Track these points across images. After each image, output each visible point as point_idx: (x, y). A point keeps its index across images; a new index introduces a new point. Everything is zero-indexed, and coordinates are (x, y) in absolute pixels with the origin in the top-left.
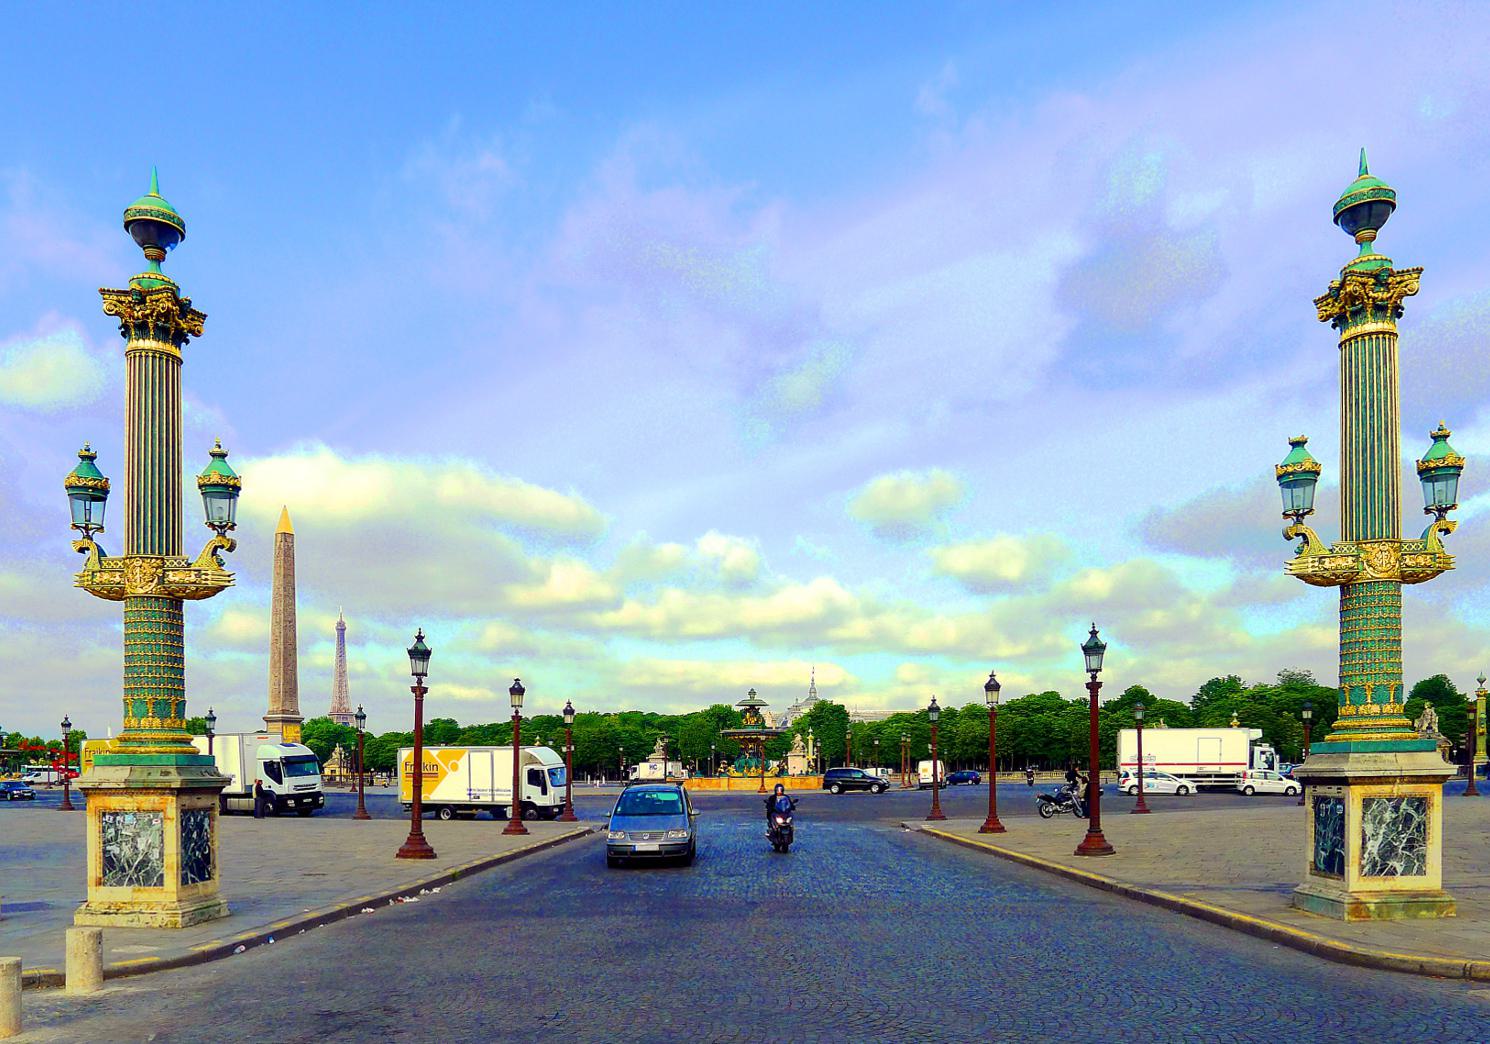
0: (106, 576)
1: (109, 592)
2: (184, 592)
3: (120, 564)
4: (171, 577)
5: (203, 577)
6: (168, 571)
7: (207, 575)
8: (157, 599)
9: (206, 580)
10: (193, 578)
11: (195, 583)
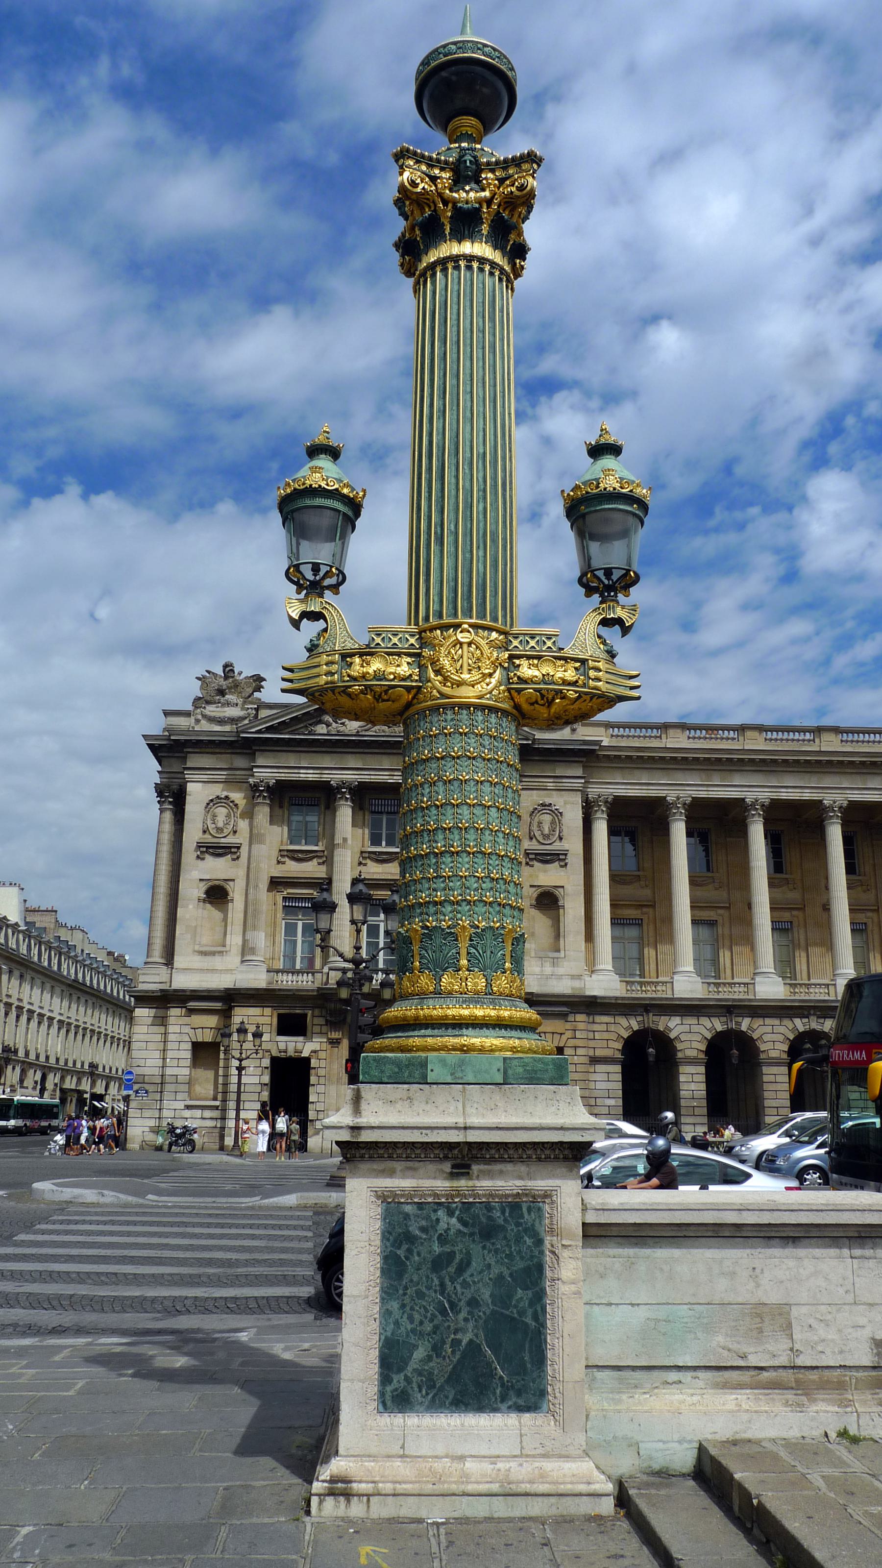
0: (376, 665)
1: (378, 698)
2: (550, 703)
3: (412, 641)
4: (526, 670)
5: (592, 673)
6: (519, 657)
7: (598, 670)
8: (492, 709)
9: (598, 679)
10: (570, 674)
11: (575, 683)
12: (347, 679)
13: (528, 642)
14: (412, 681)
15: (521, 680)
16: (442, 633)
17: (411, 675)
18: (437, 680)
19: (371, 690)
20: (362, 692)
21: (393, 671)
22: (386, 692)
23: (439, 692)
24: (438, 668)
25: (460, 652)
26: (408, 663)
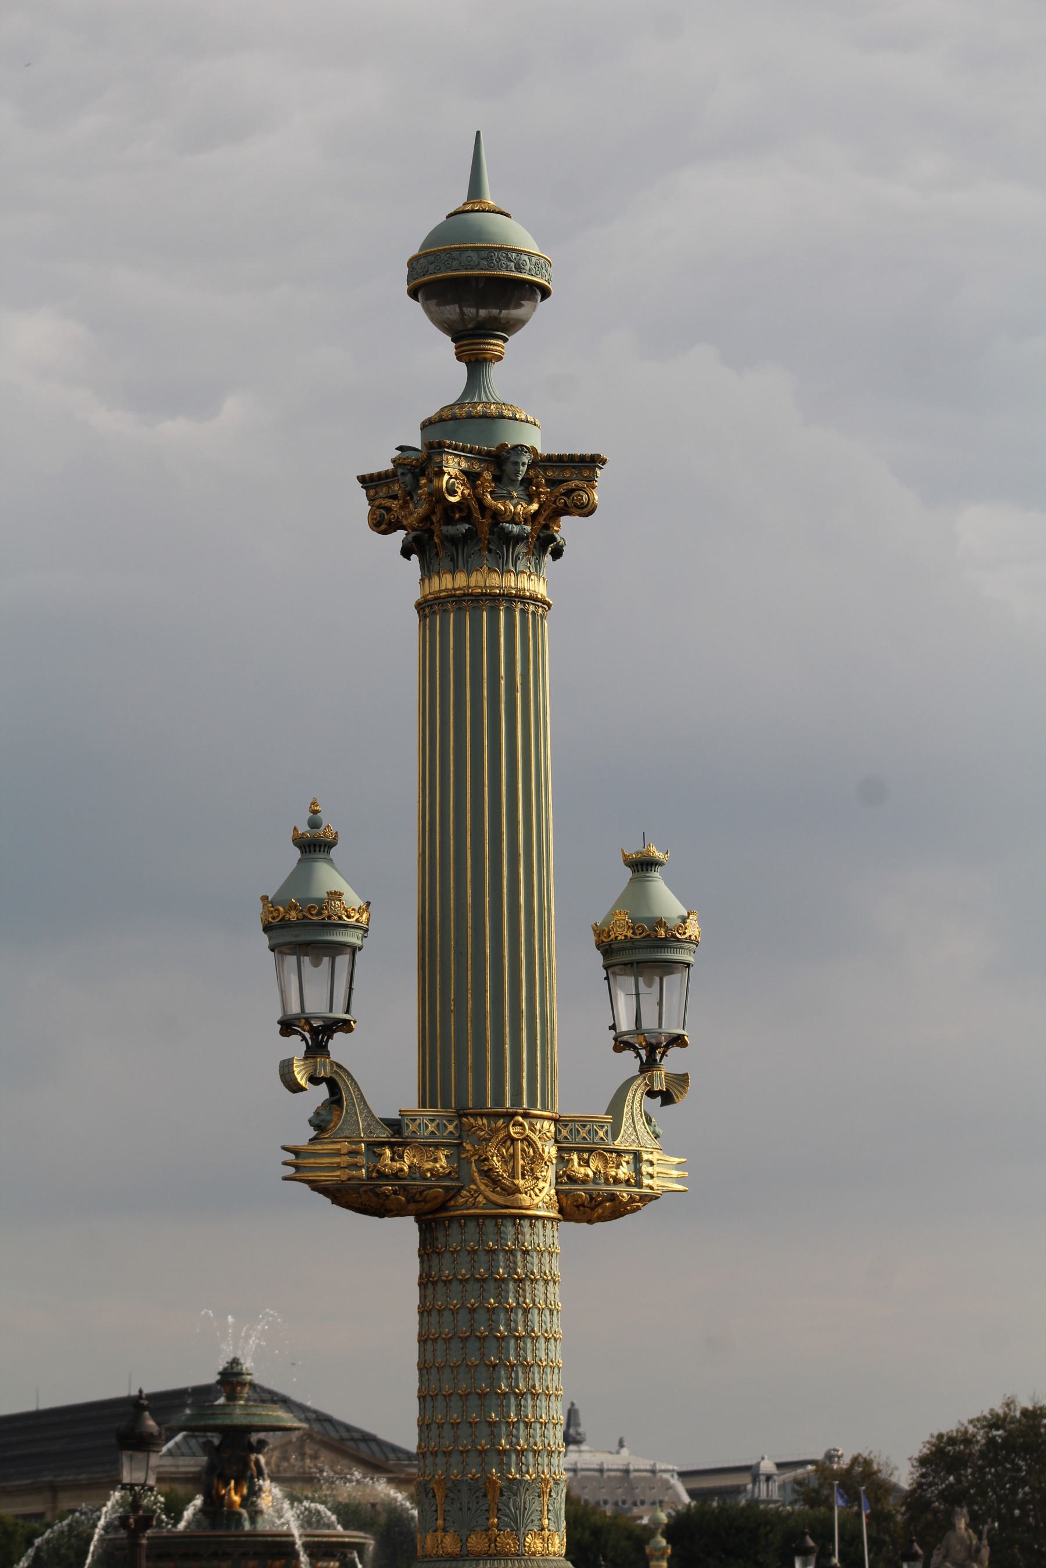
6: (570, 1150)
12: (374, 1175)
13: (578, 1131)
14: (452, 1180)
15: (572, 1180)
16: (489, 1123)
17: (450, 1173)
18: (481, 1183)
19: (405, 1190)
20: (395, 1192)
21: (429, 1167)
22: (421, 1193)
23: (485, 1197)
24: (486, 1168)
25: (511, 1150)
26: (446, 1156)
